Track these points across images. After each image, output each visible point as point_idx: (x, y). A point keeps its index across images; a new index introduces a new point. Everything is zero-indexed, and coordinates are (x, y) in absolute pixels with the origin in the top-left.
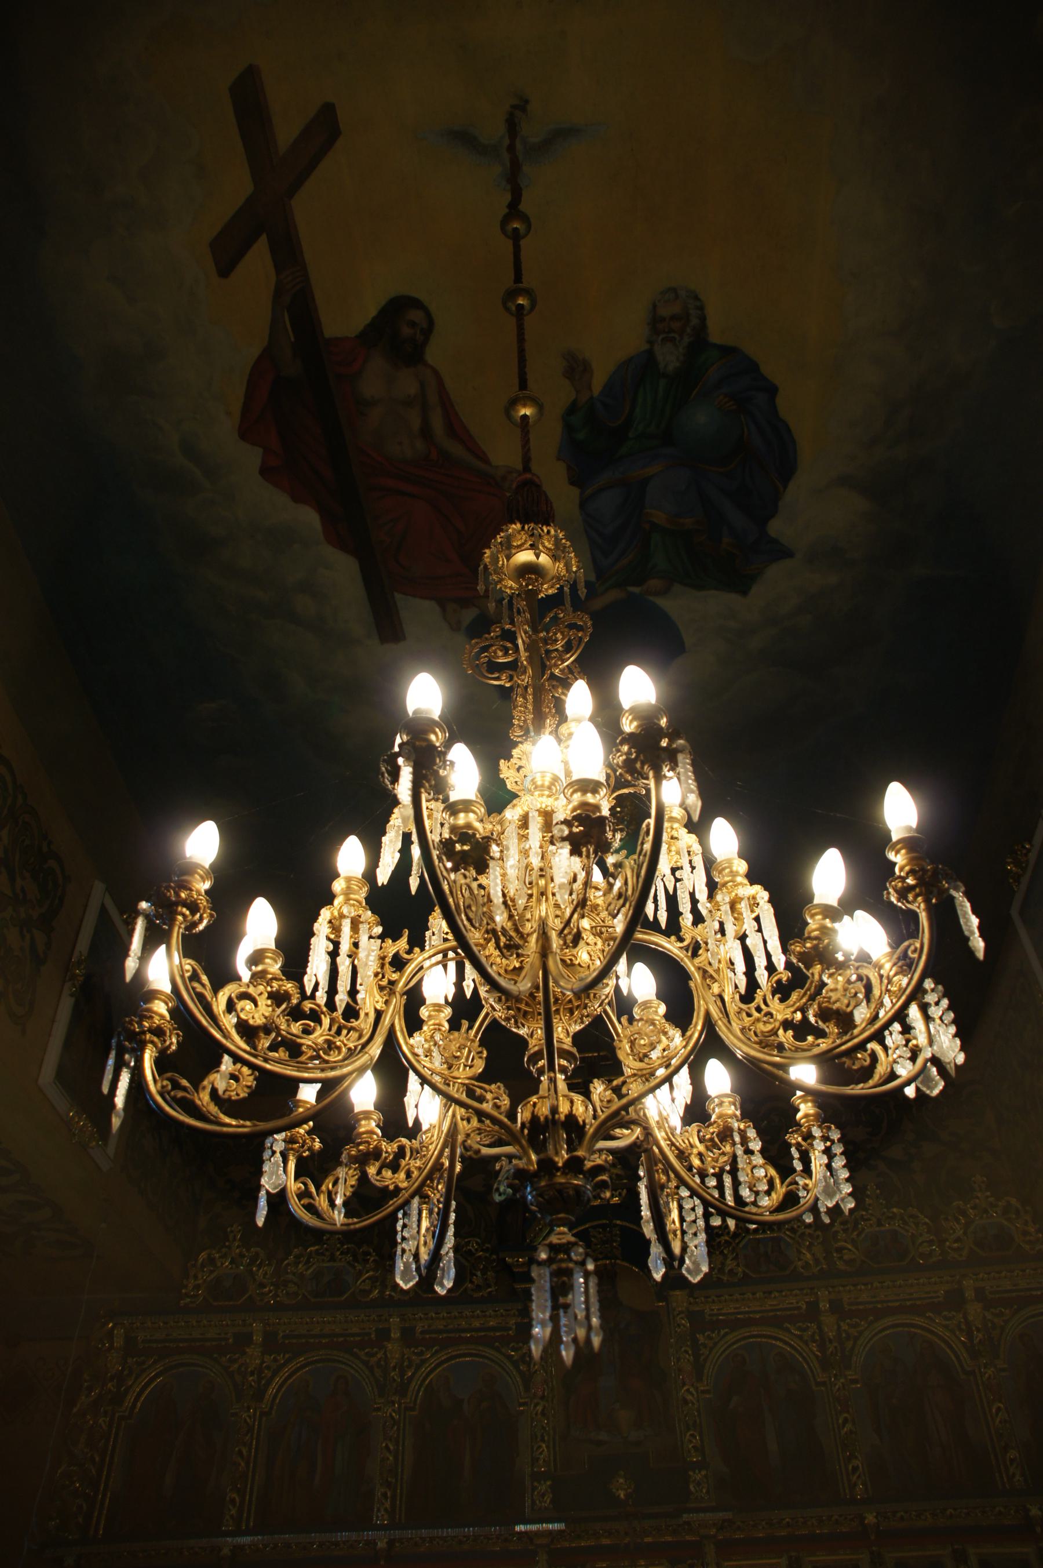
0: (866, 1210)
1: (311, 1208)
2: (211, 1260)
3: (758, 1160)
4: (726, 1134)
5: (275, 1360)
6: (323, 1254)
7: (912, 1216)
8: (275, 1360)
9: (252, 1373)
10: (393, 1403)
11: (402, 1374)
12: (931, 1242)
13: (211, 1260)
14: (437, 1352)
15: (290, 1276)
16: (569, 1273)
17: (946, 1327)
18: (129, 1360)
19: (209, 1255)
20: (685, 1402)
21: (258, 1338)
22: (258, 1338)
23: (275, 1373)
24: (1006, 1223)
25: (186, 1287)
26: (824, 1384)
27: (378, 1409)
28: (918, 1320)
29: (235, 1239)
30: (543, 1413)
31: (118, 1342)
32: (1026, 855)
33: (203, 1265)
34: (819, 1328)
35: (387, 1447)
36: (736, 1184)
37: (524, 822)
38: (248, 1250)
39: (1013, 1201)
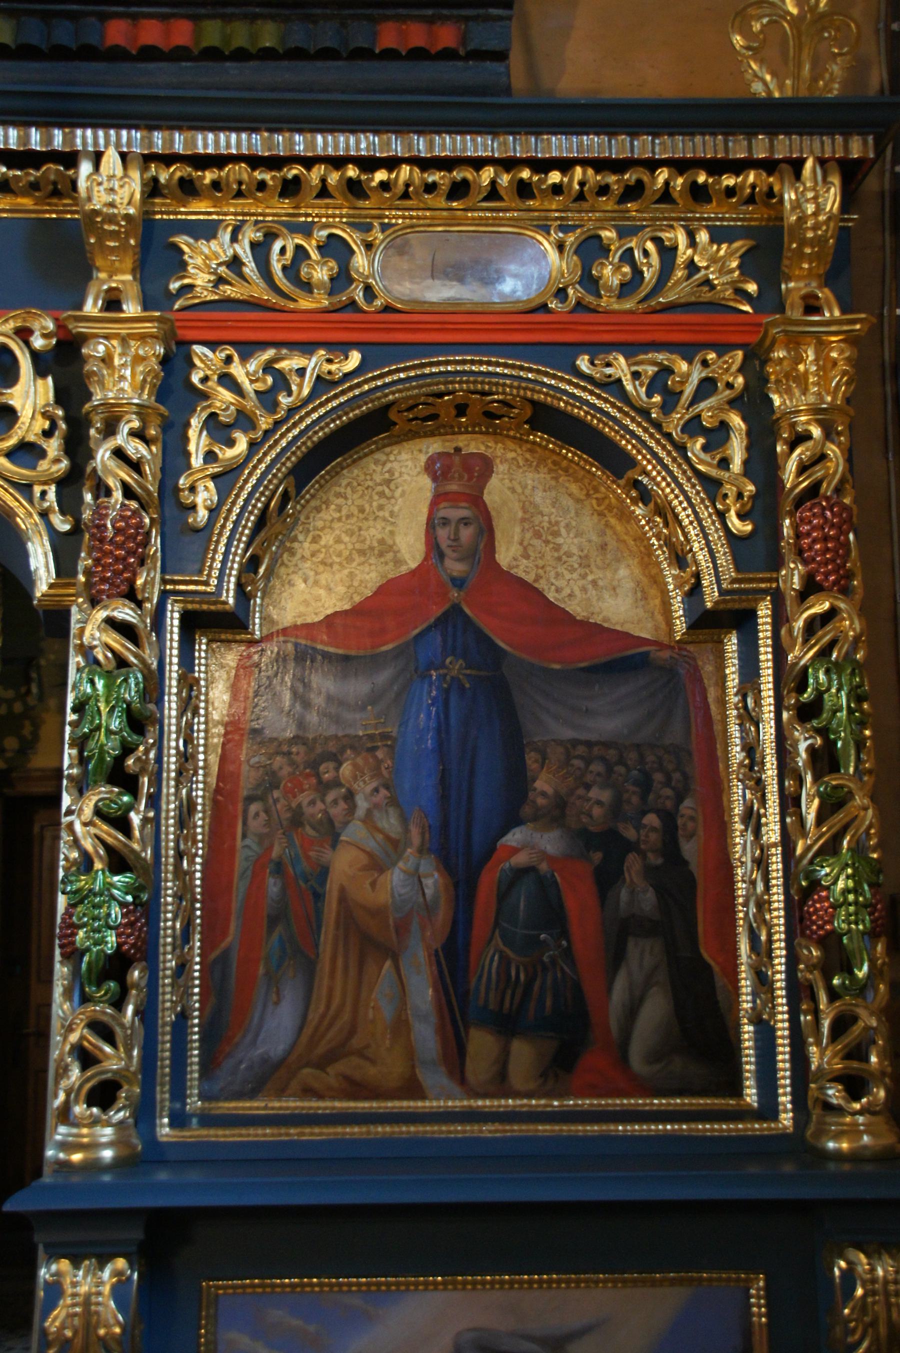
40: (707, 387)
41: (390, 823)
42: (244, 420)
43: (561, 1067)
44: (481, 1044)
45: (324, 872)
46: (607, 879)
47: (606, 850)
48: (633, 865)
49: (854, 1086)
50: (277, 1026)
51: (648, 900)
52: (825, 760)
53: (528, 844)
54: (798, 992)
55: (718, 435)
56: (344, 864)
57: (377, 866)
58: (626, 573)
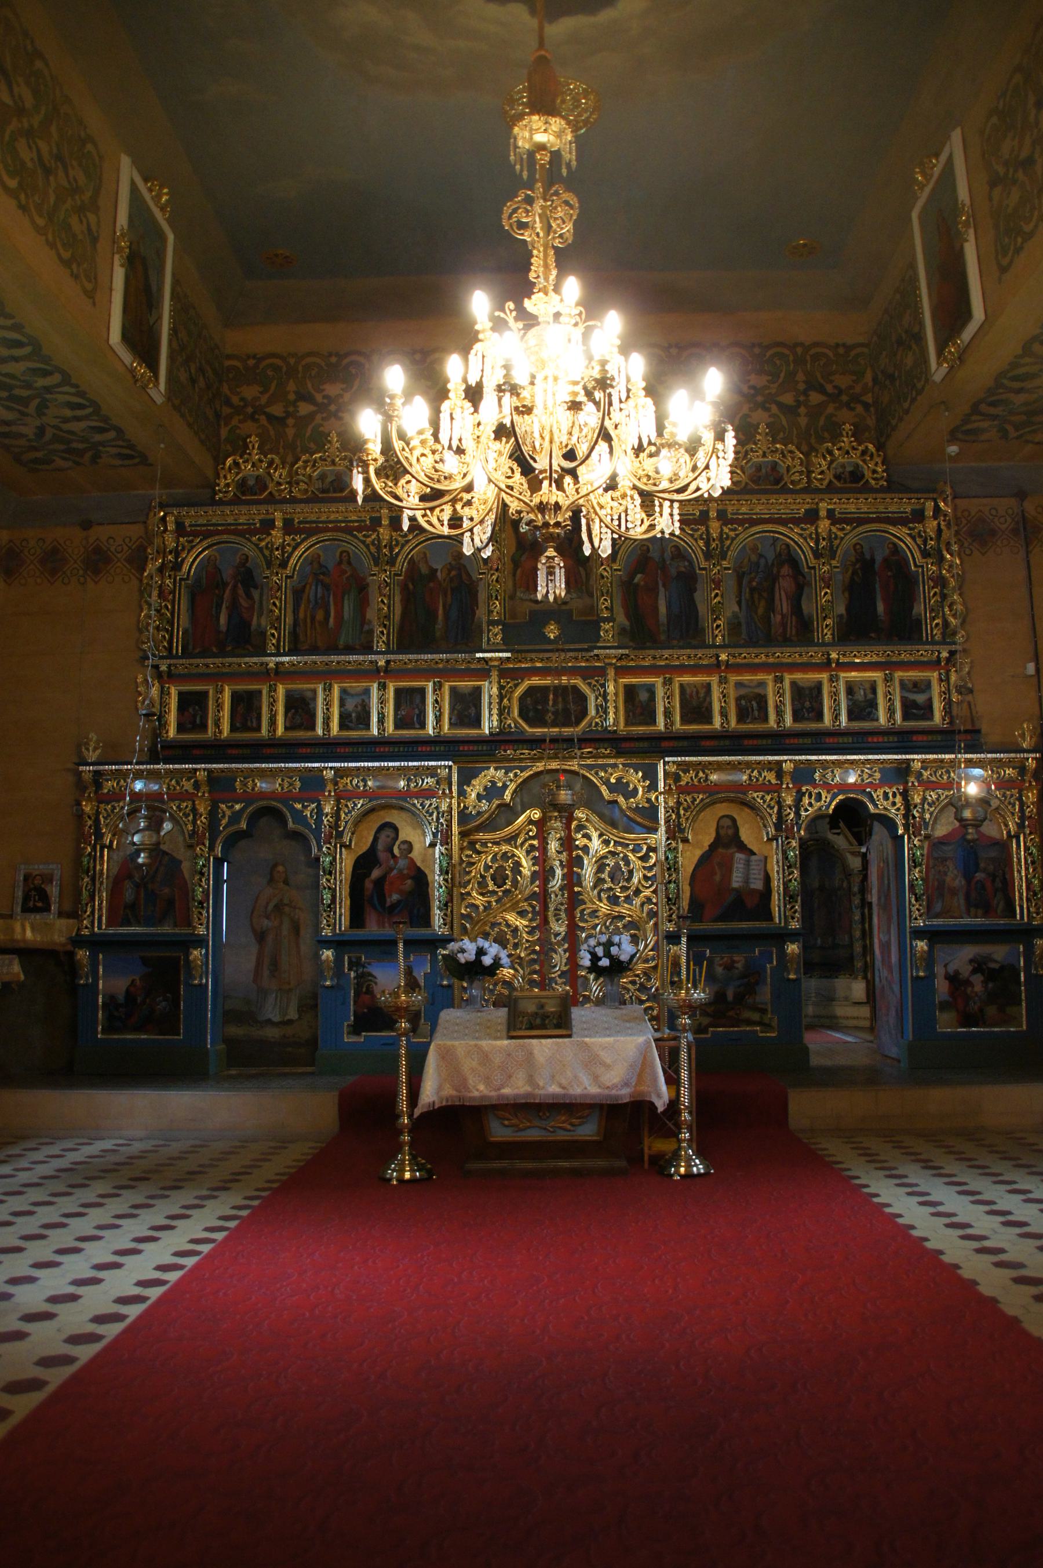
0: (755, 444)
1: (429, 523)
2: (236, 464)
3: (638, 509)
4: (624, 496)
5: (293, 539)
6: (325, 460)
7: (791, 452)
8: (293, 539)
9: (277, 549)
10: (386, 571)
11: (391, 550)
12: (801, 473)
13: (236, 464)
14: (417, 535)
15: (301, 477)
16: (554, 567)
17: (801, 535)
18: (181, 539)
19: (234, 461)
20: (603, 577)
21: (279, 523)
22: (279, 523)
23: (295, 548)
24: (861, 463)
25: (218, 485)
26: (704, 569)
27: (374, 575)
28: (781, 529)
29: (253, 448)
30: (497, 581)
31: (171, 527)
32: (932, 168)
33: (230, 469)
34: (707, 530)
35: (382, 601)
36: (627, 521)
37: (546, 378)
38: (265, 457)
39: (871, 446)
40: (1012, 796)
41: (955, 872)
42: (934, 802)
43: (986, 914)
44: (973, 910)
45: (944, 881)
46: (993, 881)
47: (993, 877)
48: (998, 880)
49: (1038, 914)
50: (938, 907)
51: (1000, 885)
52: (1033, 862)
53: (979, 876)
54: (1028, 900)
55: (1014, 805)
56: (948, 879)
57: (954, 879)
58: (995, 827)
